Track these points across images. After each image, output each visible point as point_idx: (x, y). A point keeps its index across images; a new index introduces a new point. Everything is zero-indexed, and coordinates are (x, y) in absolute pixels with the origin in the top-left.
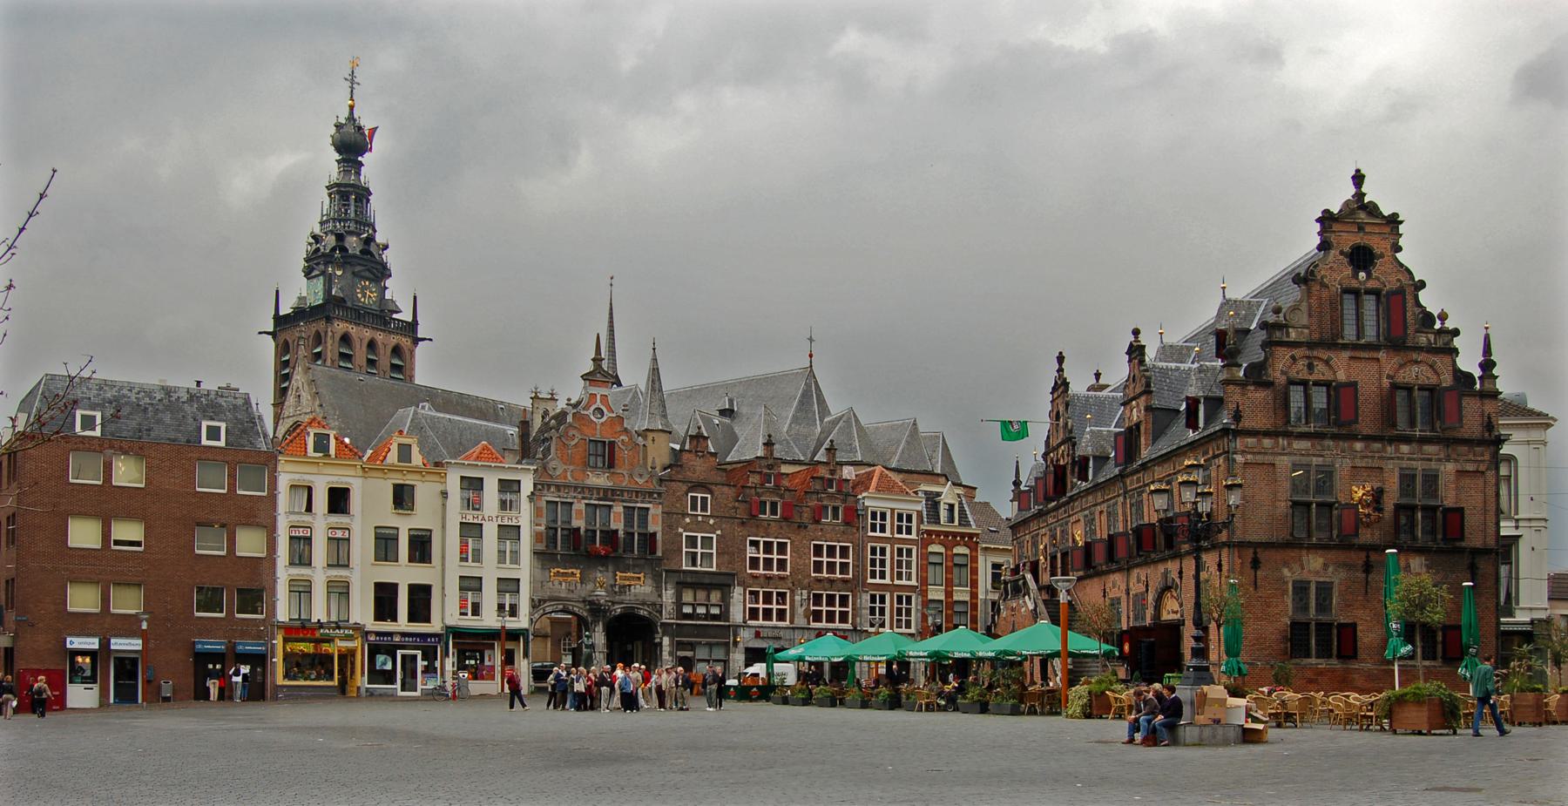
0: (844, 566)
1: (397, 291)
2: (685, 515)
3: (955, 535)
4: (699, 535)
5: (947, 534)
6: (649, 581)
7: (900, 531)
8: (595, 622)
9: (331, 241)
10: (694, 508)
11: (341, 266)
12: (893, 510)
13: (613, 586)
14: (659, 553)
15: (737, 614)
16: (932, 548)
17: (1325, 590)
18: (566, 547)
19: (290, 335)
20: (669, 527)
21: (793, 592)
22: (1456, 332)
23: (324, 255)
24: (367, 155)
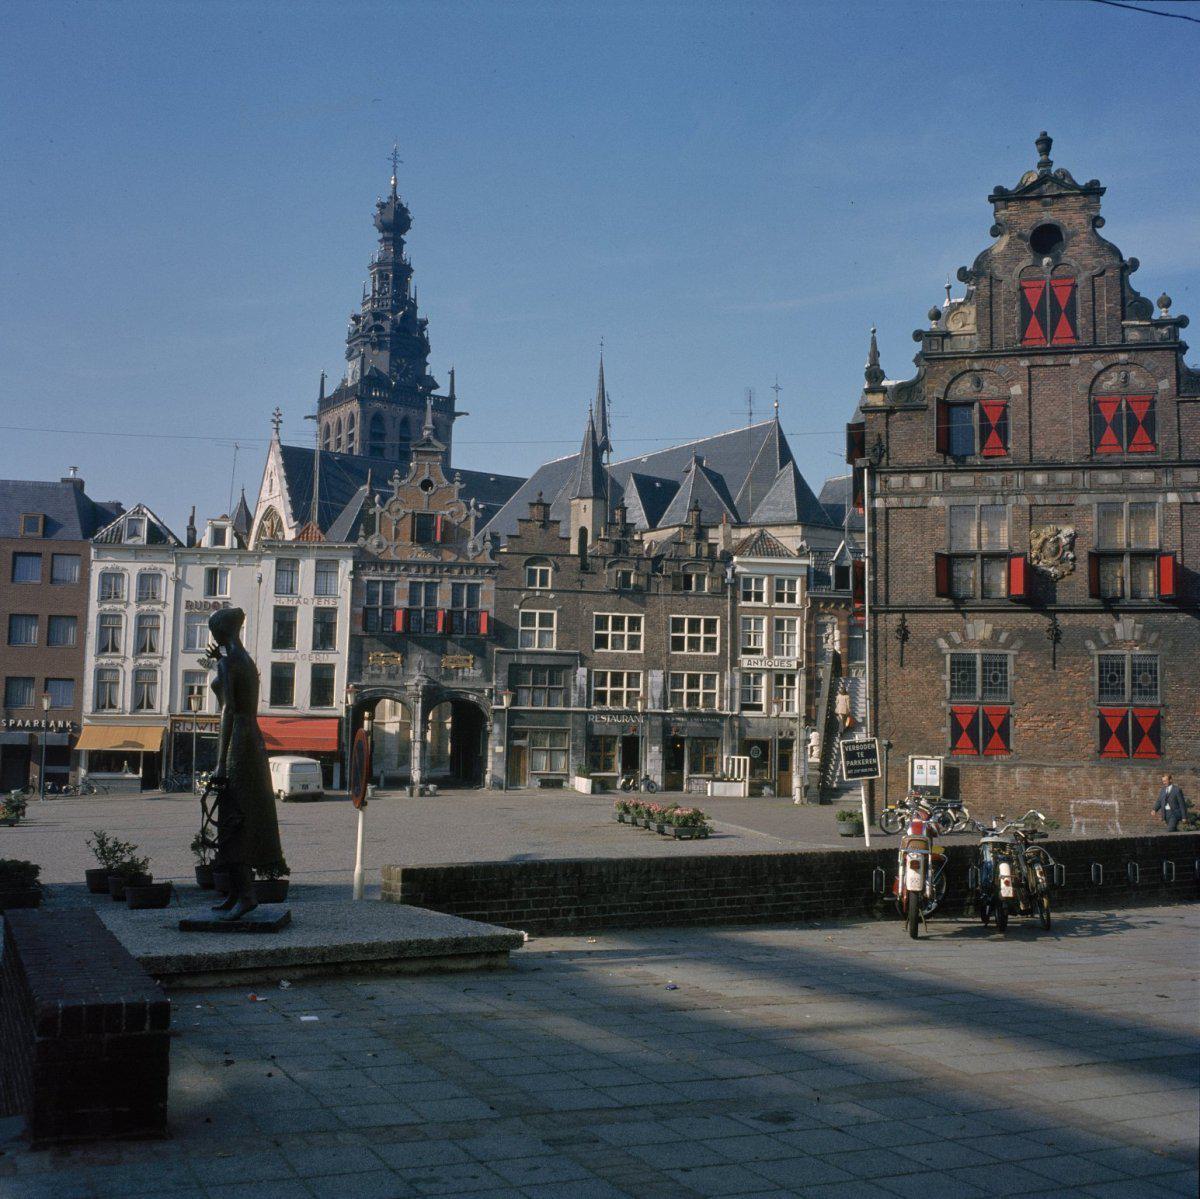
1: (436, 366)
2: (520, 590)
4: (538, 612)
7: (780, 598)
10: (532, 582)
11: (378, 345)
17: (995, 667)
19: (331, 418)
21: (646, 672)
22: (1182, 322)
24: (408, 232)
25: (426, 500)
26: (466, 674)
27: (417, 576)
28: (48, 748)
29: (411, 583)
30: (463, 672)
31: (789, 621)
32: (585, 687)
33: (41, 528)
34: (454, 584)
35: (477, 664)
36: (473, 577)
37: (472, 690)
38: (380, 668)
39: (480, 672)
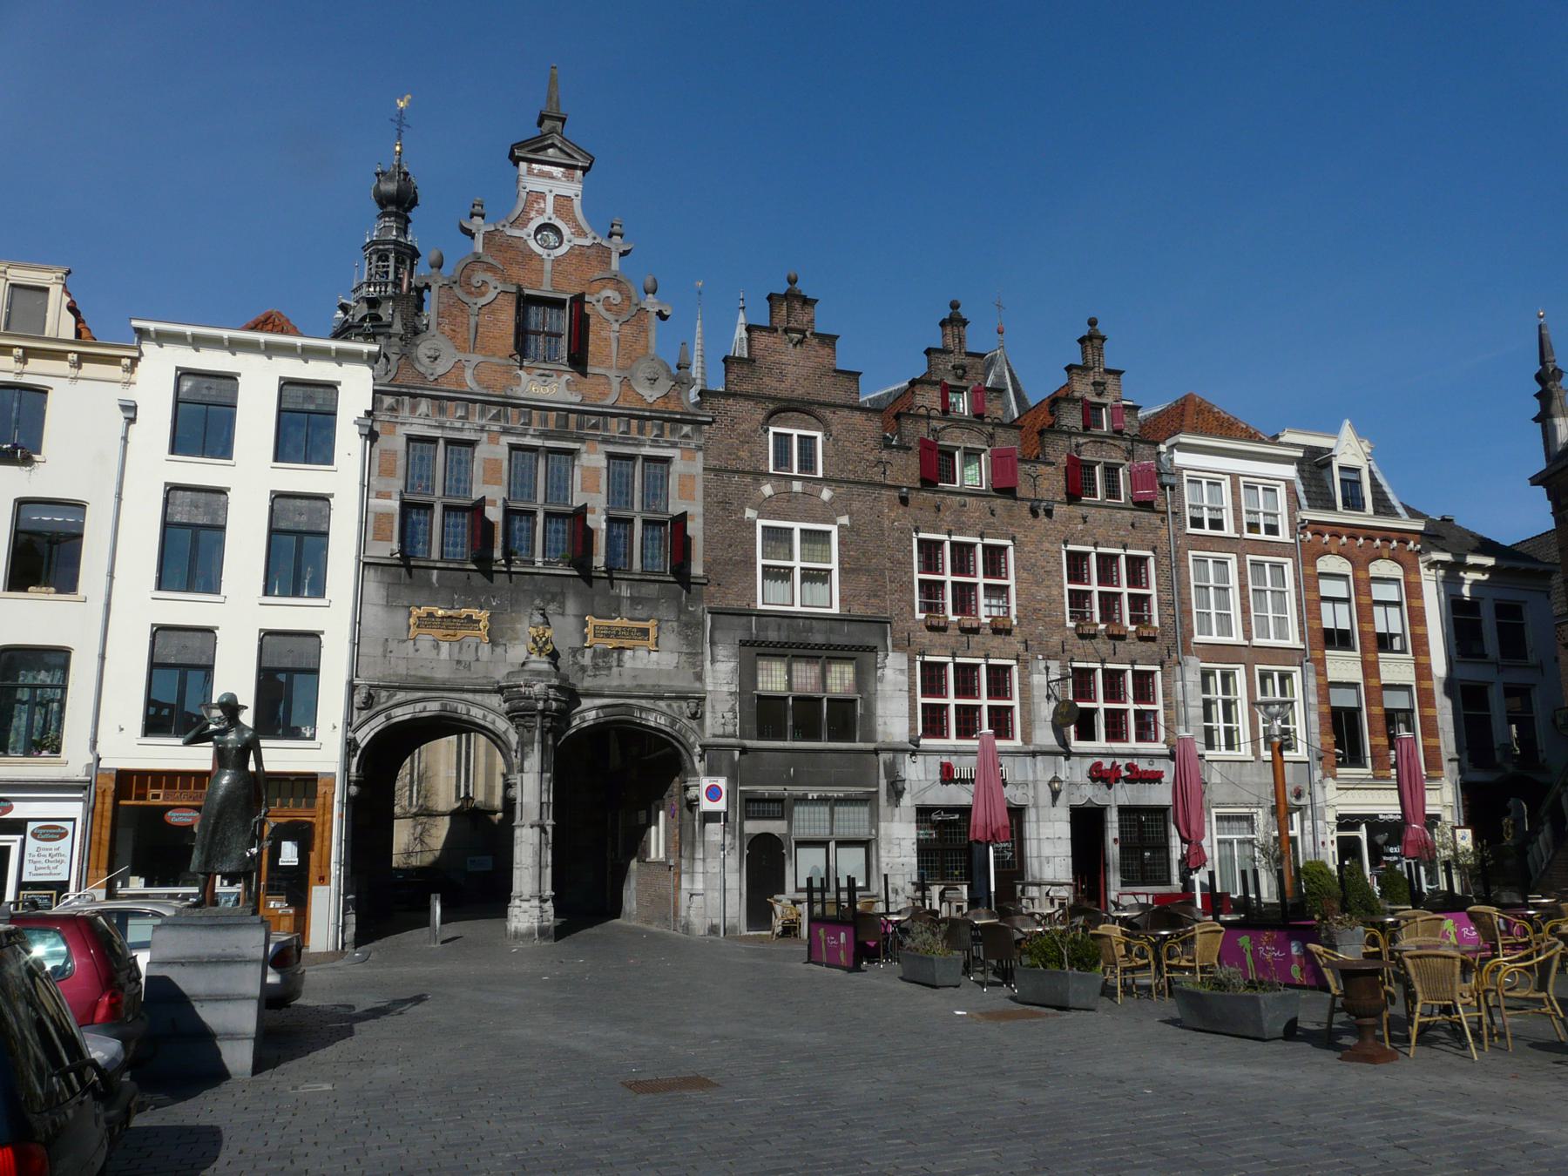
0: (1139, 602)
2: (760, 475)
3: (1370, 532)
4: (797, 527)
5: (1354, 531)
6: (671, 640)
7: (1253, 527)
8: (524, 744)
9: (363, 310)
12: (1235, 477)
13: (574, 652)
14: (697, 569)
15: (894, 716)
16: (1328, 564)
18: (446, 550)
20: (723, 507)
23: (351, 327)
25: (548, 267)
27: (525, 435)
31: (1273, 565)
34: (611, 456)
36: (655, 443)
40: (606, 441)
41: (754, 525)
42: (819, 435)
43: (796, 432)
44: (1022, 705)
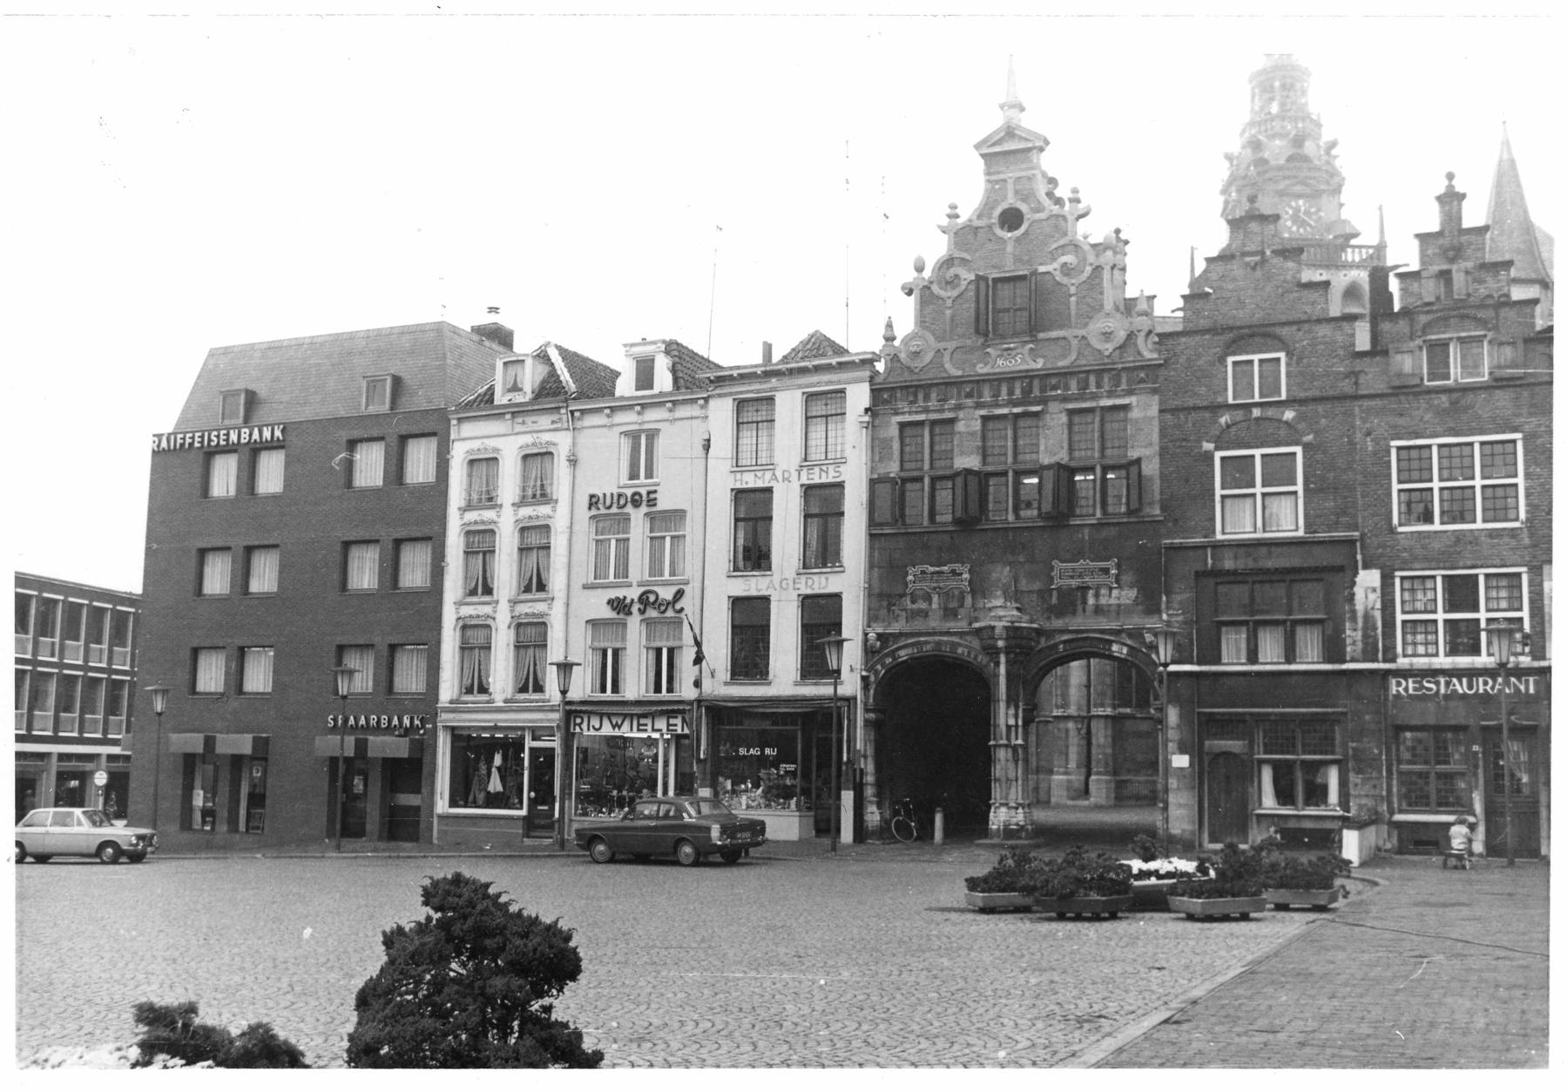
4: (1257, 453)
26: (1103, 601)
28: (385, 760)
29: (985, 419)
30: (1097, 596)
32: (1378, 615)
33: (388, 401)
35: (1127, 578)
36: (1111, 394)
37: (1118, 632)
38: (928, 599)
39: (1133, 593)
40: (1065, 399)
41: (1209, 457)
42: (1282, 355)
43: (1256, 358)
44: (1532, 616)
